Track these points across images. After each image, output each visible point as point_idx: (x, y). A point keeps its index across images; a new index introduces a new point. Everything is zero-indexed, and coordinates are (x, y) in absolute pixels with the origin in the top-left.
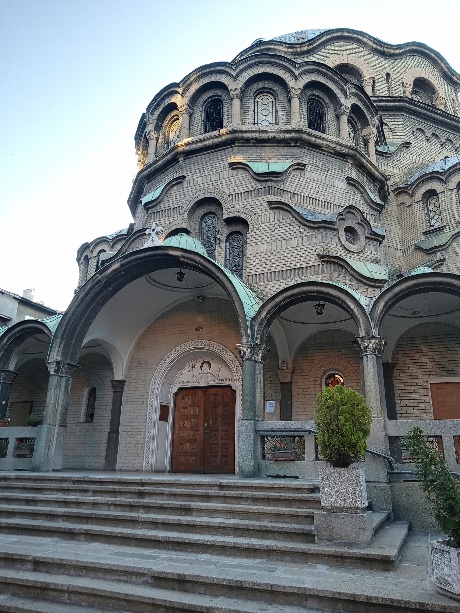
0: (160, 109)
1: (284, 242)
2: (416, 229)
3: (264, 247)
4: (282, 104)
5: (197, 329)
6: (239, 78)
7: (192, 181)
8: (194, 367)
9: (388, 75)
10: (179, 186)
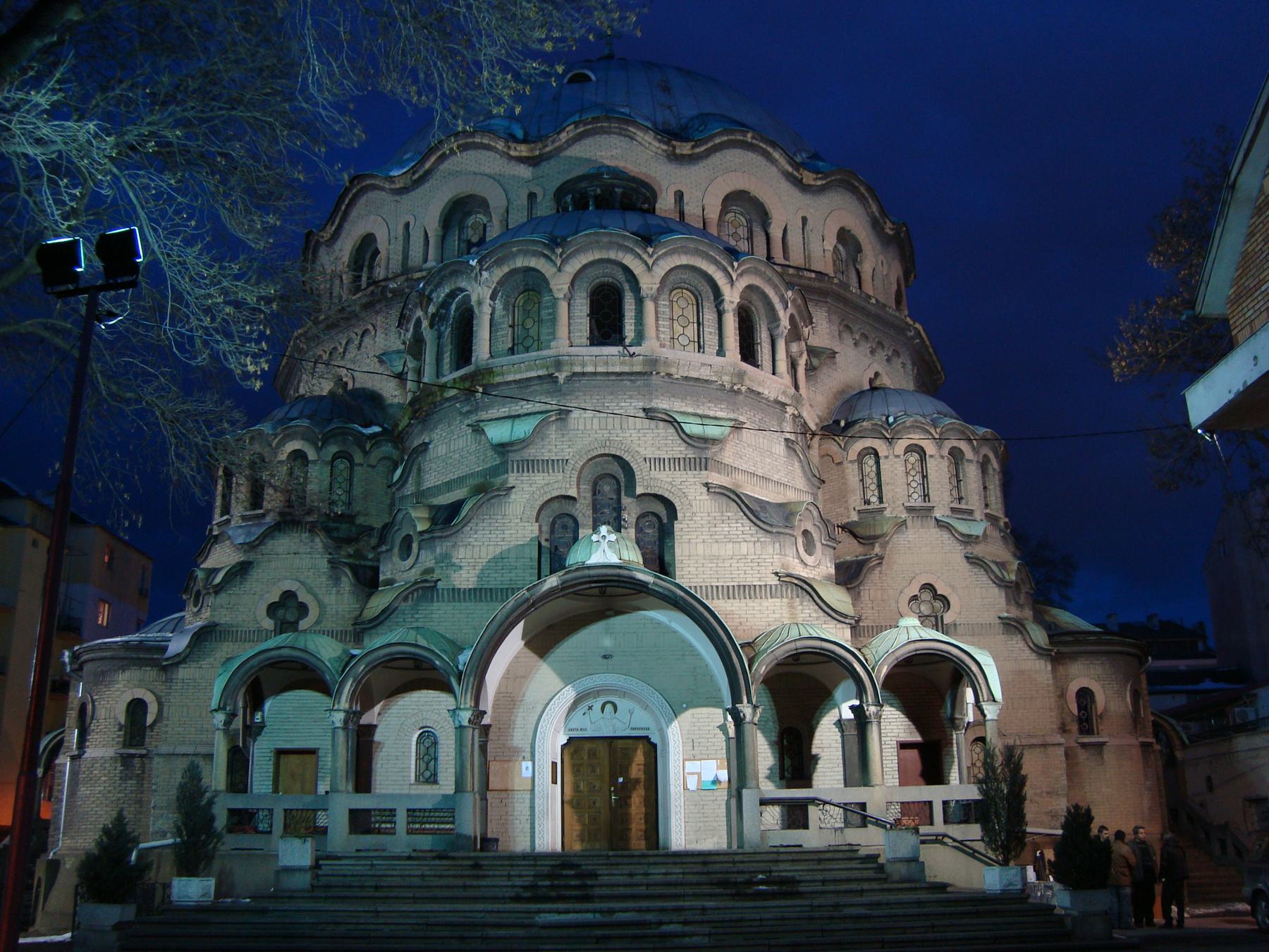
0: (506, 269)
1: (730, 546)
2: (846, 502)
3: (700, 547)
4: (709, 316)
5: (605, 657)
6: (655, 268)
7: (582, 421)
8: (590, 708)
9: (804, 220)
10: (559, 423)
